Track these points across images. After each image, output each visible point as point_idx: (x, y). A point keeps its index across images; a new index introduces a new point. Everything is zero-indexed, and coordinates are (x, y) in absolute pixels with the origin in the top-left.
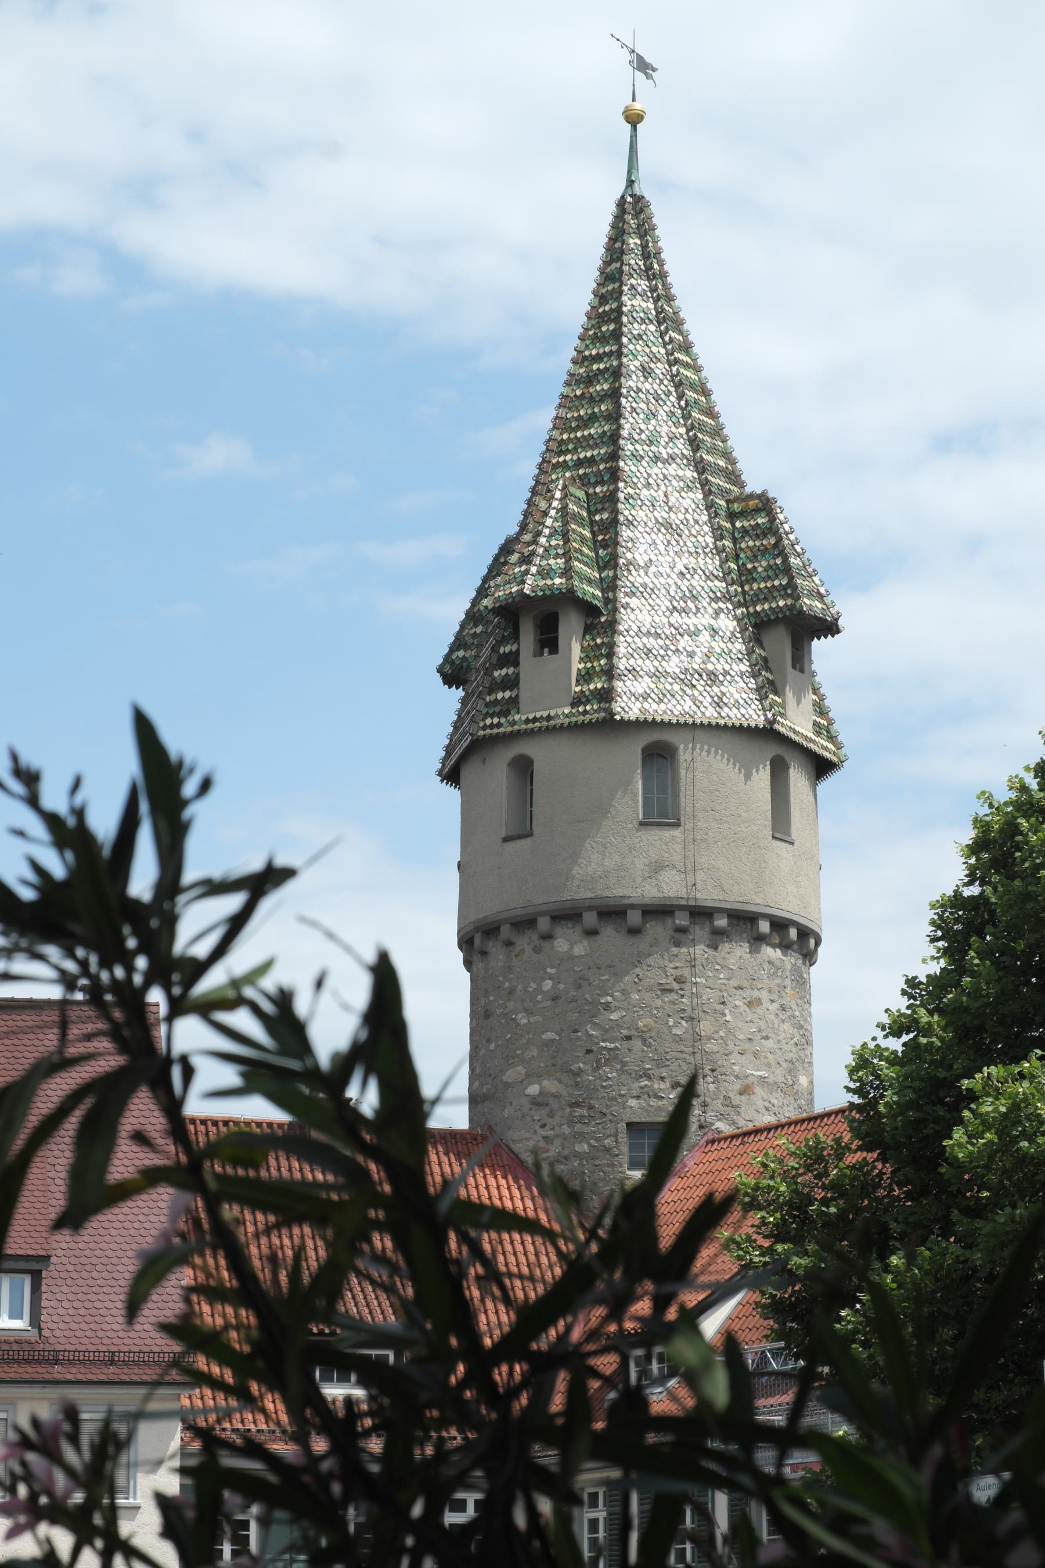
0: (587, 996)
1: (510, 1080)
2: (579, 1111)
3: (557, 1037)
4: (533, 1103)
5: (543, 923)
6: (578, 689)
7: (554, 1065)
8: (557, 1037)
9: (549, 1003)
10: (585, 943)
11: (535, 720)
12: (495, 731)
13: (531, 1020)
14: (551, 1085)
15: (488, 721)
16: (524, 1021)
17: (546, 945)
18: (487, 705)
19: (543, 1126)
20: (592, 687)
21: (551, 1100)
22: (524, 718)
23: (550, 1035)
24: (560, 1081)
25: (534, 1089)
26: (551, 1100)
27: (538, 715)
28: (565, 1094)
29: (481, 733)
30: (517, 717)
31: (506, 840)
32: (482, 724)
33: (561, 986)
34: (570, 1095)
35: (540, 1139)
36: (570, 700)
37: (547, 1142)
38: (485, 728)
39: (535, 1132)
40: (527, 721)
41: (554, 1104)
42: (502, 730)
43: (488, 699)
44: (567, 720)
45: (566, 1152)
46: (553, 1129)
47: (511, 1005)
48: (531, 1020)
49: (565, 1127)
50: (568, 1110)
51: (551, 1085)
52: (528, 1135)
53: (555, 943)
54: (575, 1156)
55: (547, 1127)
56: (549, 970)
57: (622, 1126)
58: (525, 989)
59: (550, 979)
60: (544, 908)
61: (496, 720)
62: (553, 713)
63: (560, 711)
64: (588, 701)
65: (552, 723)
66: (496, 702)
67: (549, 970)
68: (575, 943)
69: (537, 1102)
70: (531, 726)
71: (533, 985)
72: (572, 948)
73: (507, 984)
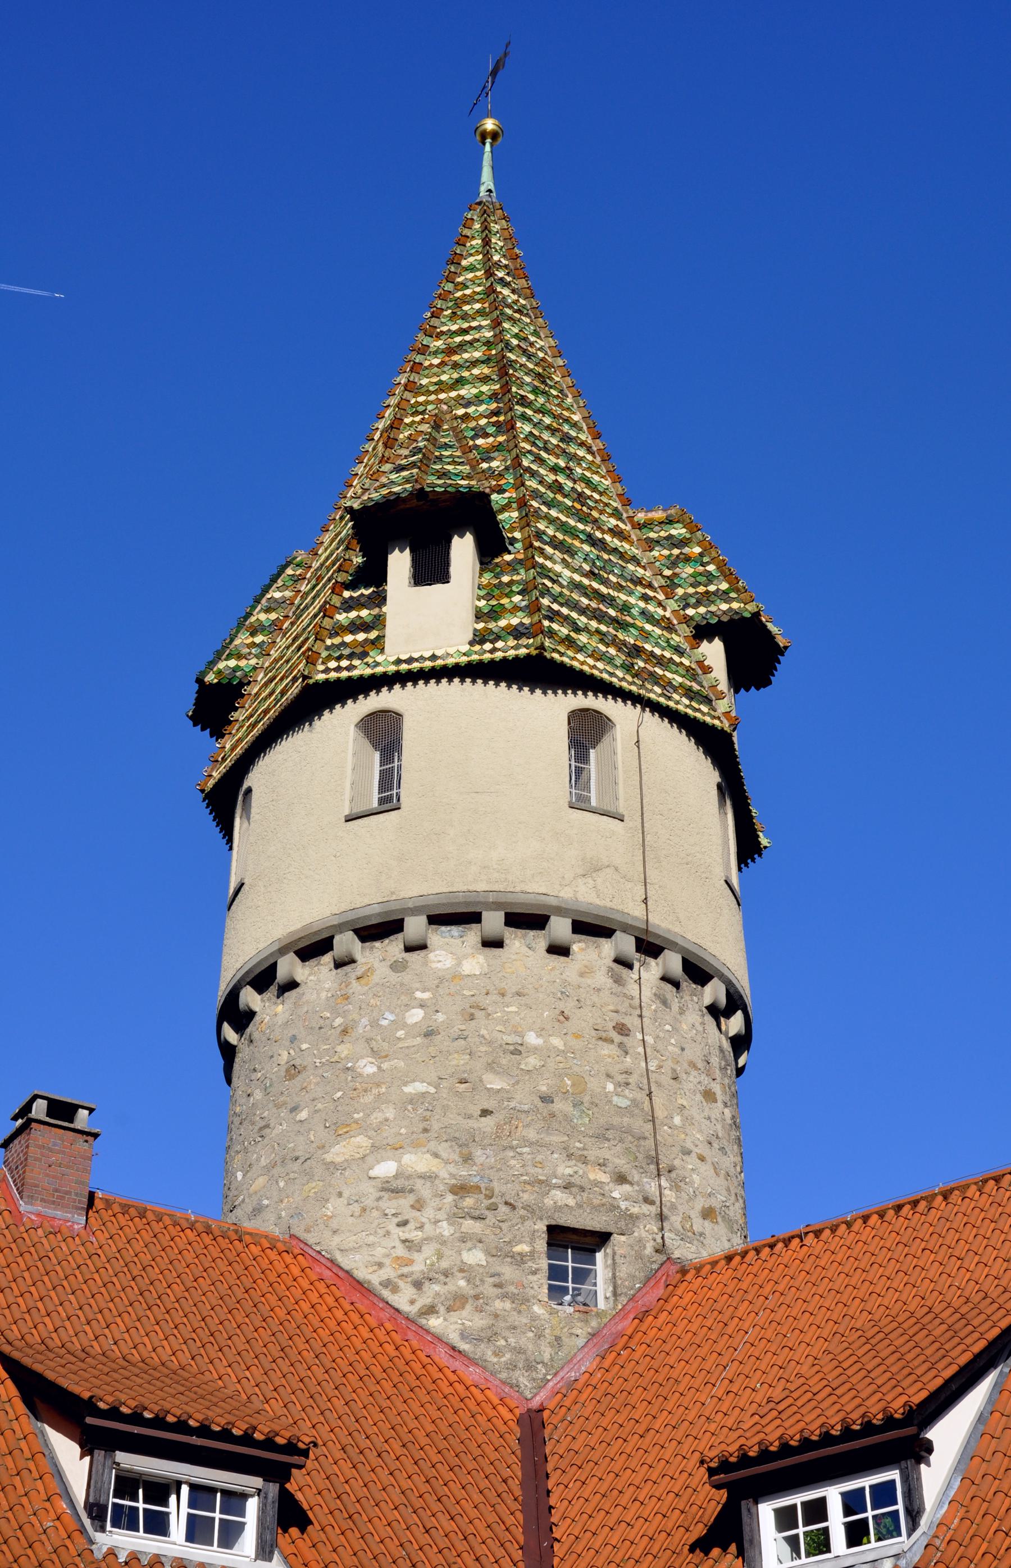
0: (483, 1032)
1: (339, 1159)
2: (469, 1202)
3: (432, 1090)
4: (383, 1189)
5: (415, 926)
6: (480, 626)
7: (426, 1130)
8: (432, 1090)
9: (419, 1040)
10: (481, 958)
11: (410, 660)
12: (345, 674)
13: (385, 1066)
14: (417, 1161)
15: (333, 664)
16: (371, 1069)
17: (415, 957)
18: (327, 648)
19: (404, 1223)
20: (503, 623)
21: (419, 1184)
22: (392, 659)
23: (419, 1087)
24: (436, 1155)
25: (386, 1169)
26: (419, 1184)
27: (416, 655)
28: (443, 1174)
29: (321, 677)
30: (380, 658)
31: (348, 820)
32: (321, 668)
33: (440, 1017)
34: (452, 1176)
35: (398, 1244)
36: (470, 636)
37: (409, 1248)
38: (327, 670)
39: (388, 1233)
40: (399, 662)
41: (424, 1190)
42: (356, 673)
43: (329, 642)
44: (464, 660)
45: (444, 1264)
46: (421, 1227)
47: (344, 1050)
48: (385, 1066)
49: (444, 1224)
50: (450, 1198)
51: (417, 1161)
52: (371, 1239)
53: (432, 956)
54: (461, 1271)
55: (411, 1226)
56: (419, 995)
57: (541, 1227)
58: (374, 1024)
59: (422, 1006)
60: (420, 902)
61: (345, 663)
62: (438, 653)
63: (451, 651)
64: (498, 638)
65: (439, 662)
66: (343, 644)
67: (419, 995)
68: (466, 956)
69: (391, 1188)
70: (404, 667)
71: (392, 1017)
72: (459, 964)
73: (339, 1021)
